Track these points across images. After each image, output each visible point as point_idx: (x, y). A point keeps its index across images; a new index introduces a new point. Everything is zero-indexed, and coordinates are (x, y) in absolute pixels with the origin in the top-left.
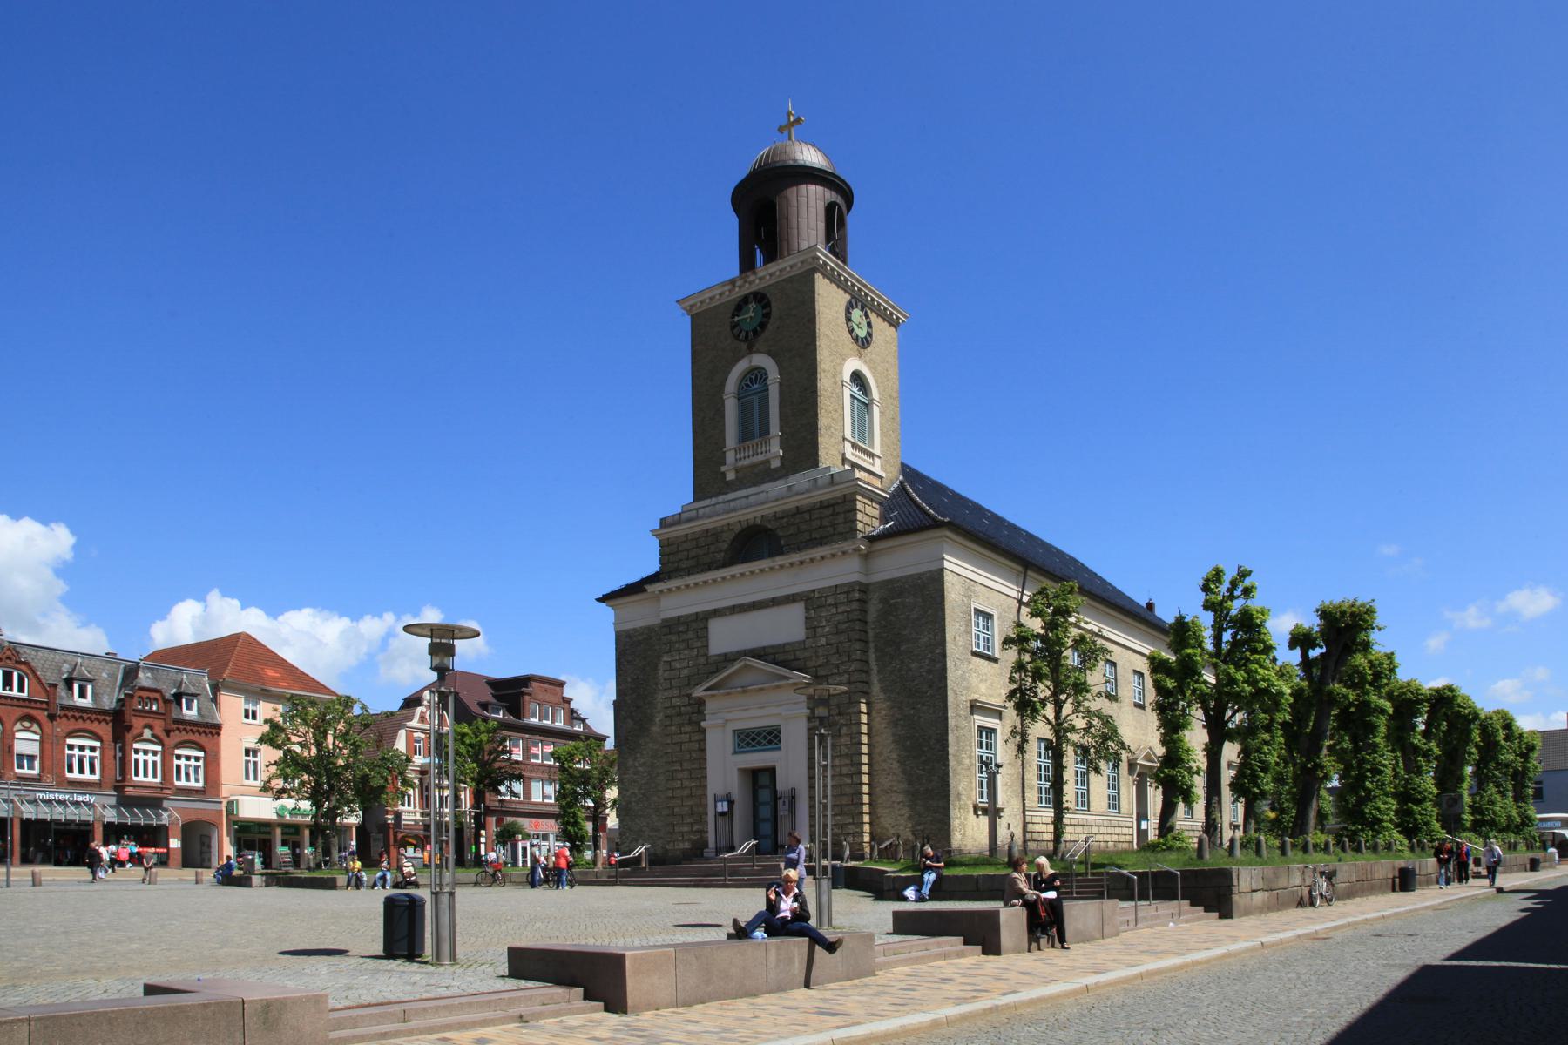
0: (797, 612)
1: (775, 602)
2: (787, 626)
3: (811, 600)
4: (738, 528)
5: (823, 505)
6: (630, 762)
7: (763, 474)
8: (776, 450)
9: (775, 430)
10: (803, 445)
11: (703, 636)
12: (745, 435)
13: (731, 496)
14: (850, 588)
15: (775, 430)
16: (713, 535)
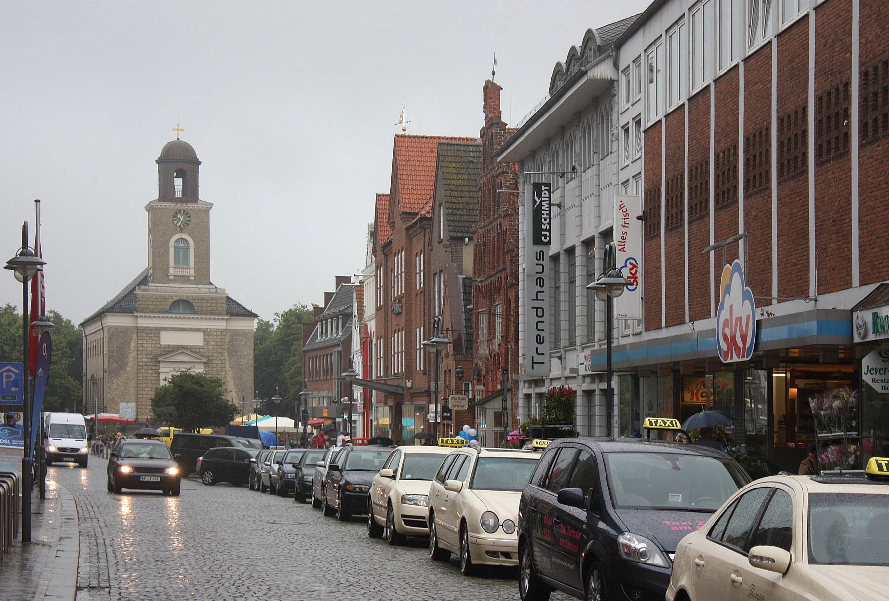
0: (201, 335)
1: (191, 330)
2: (196, 340)
3: (205, 331)
4: (176, 299)
5: (212, 299)
6: (115, 381)
7: (185, 279)
8: (192, 272)
9: (192, 264)
10: (203, 274)
11: (157, 335)
12: (176, 261)
13: (172, 285)
14: (222, 331)
15: (192, 264)
16: (165, 298)
